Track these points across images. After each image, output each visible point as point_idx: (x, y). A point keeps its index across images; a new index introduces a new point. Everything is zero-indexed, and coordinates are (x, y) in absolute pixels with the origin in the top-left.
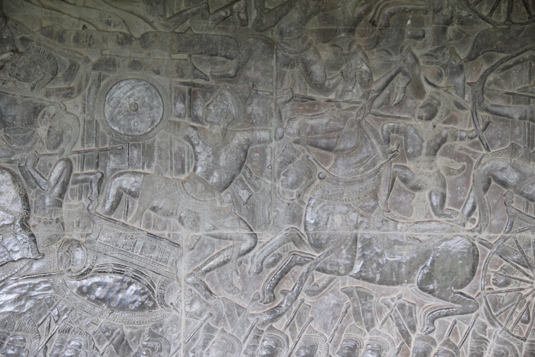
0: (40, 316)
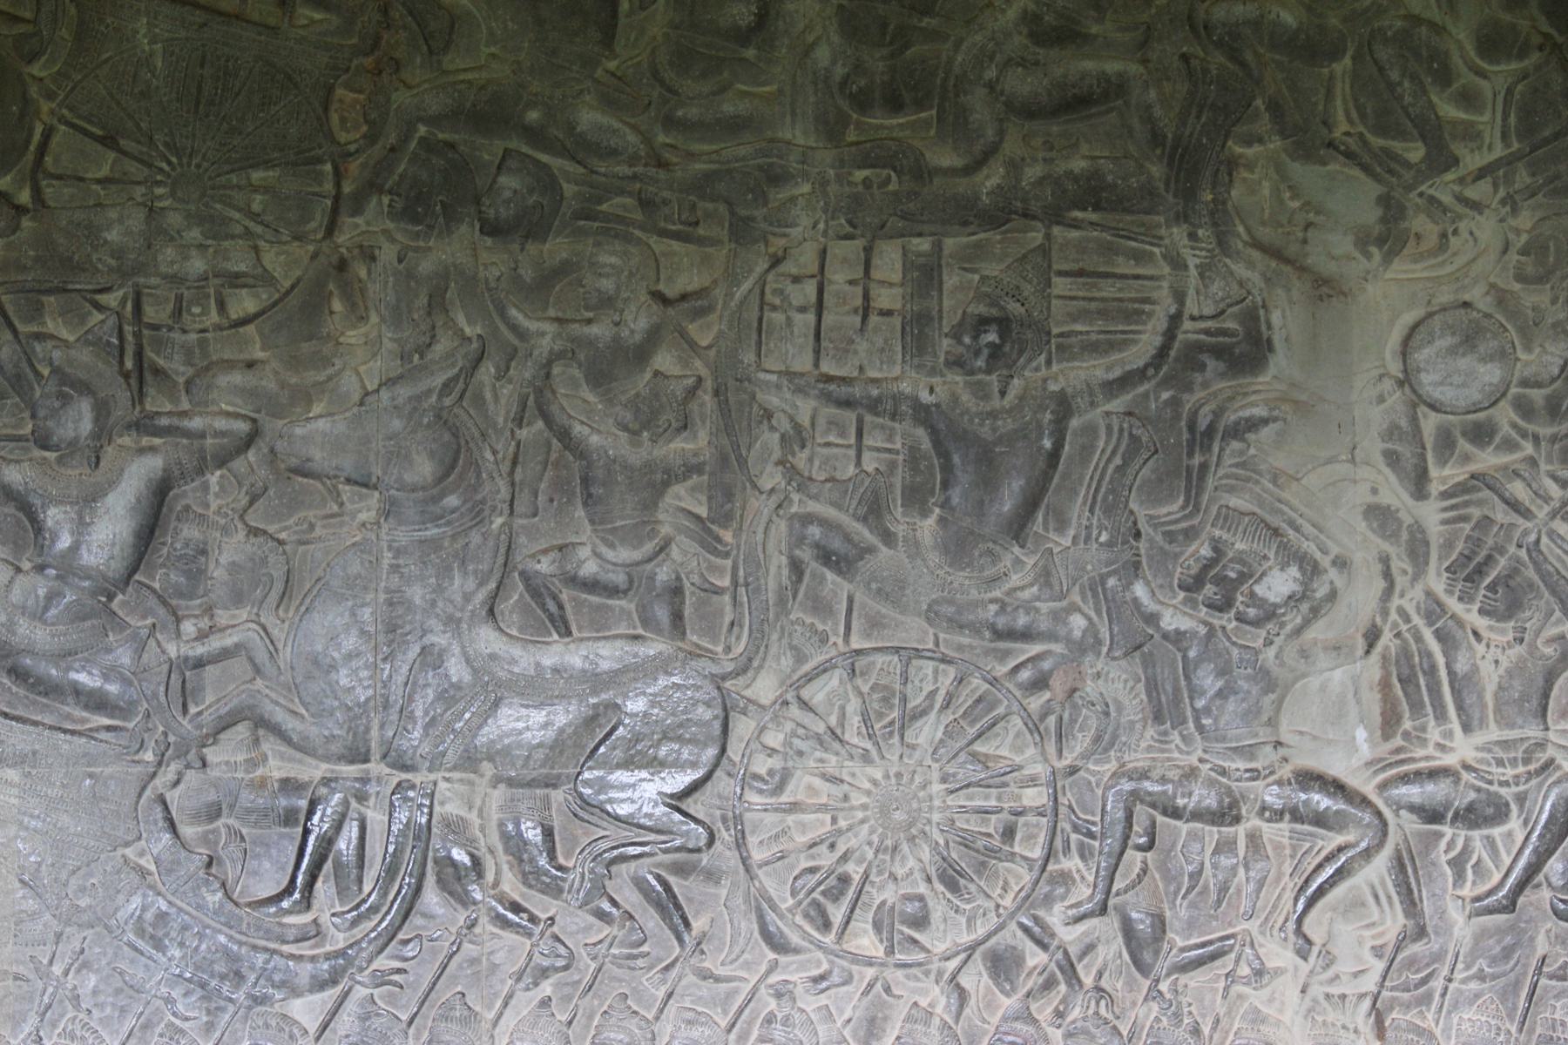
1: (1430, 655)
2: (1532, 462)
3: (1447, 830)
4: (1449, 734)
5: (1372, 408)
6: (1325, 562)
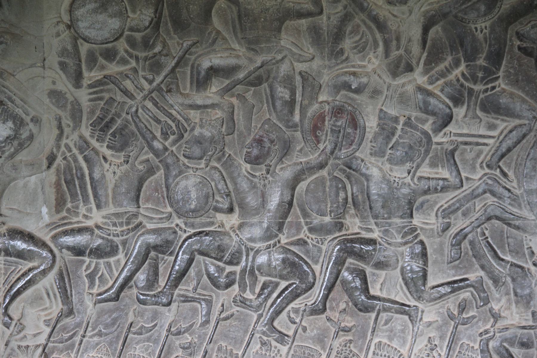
1: (81, 169)
2: (135, 70)
3: (87, 260)
4: (90, 210)
5: (52, 38)
6: (28, 119)
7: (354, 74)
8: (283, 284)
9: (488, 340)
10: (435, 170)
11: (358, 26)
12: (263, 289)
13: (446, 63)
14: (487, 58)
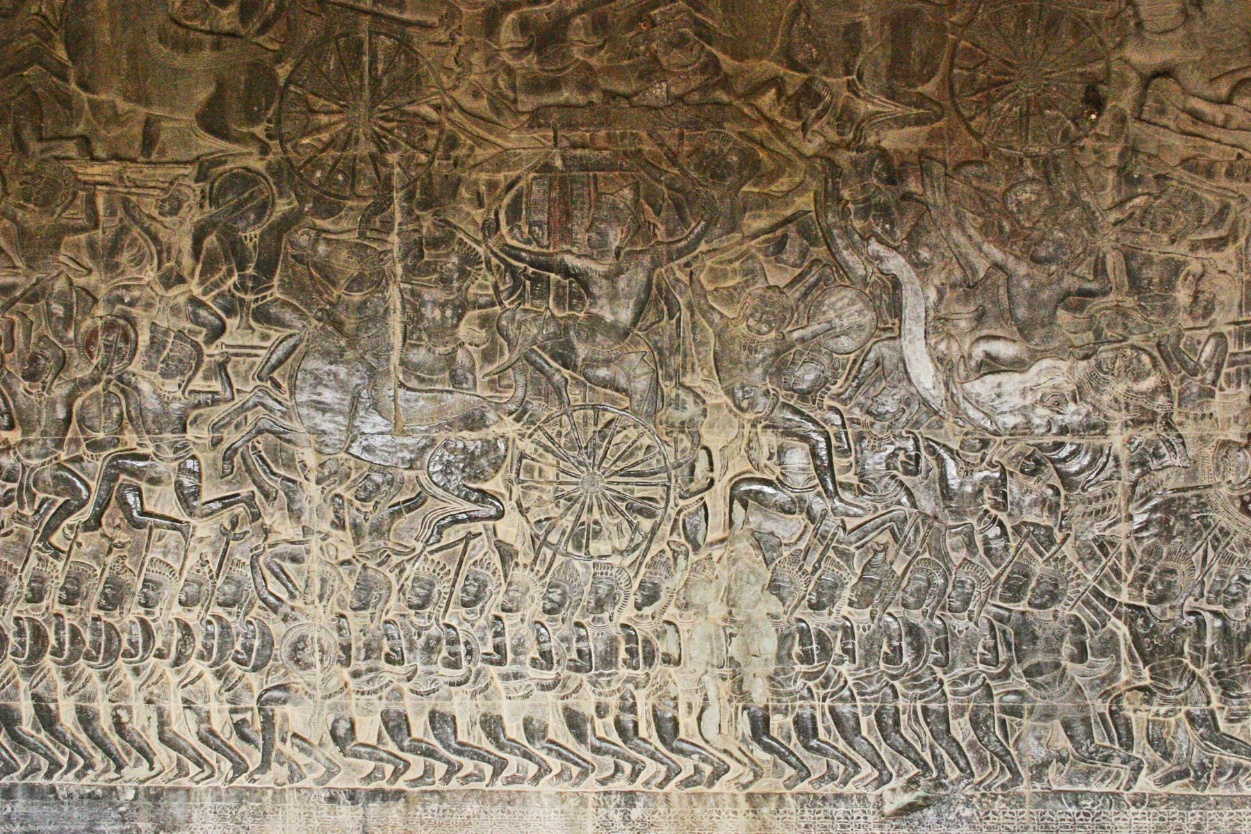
0: (1195, 540)
7: (126, 287)
8: (61, 500)
9: (258, 556)
10: (209, 383)
11: (136, 239)
12: (40, 506)
13: (222, 273)
14: (257, 267)
